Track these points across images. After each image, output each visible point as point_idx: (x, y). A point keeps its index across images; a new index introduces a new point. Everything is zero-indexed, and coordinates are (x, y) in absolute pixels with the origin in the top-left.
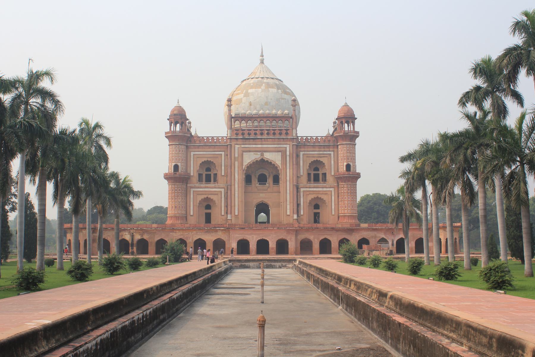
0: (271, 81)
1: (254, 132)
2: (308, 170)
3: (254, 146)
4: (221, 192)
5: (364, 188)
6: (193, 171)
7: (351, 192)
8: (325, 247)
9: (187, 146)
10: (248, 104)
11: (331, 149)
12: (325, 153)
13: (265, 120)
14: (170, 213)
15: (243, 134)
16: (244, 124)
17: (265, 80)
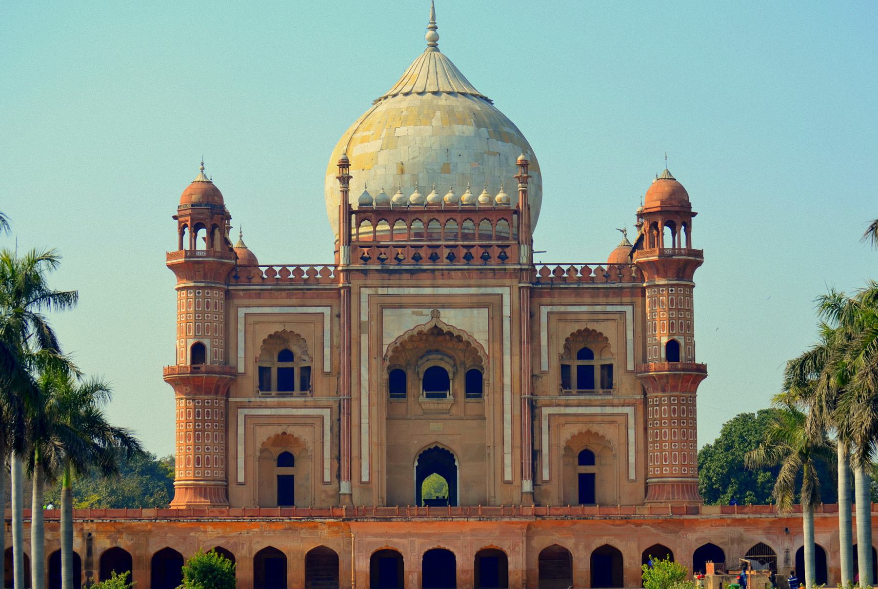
0: (459, 103)
1: (412, 251)
2: (561, 357)
3: (413, 291)
4: (322, 418)
6: (245, 359)
7: (679, 419)
10: (394, 170)
11: (626, 300)
12: (609, 308)
13: (442, 218)
14: (181, 475)
16: (383, 227)
17: (443, 100)
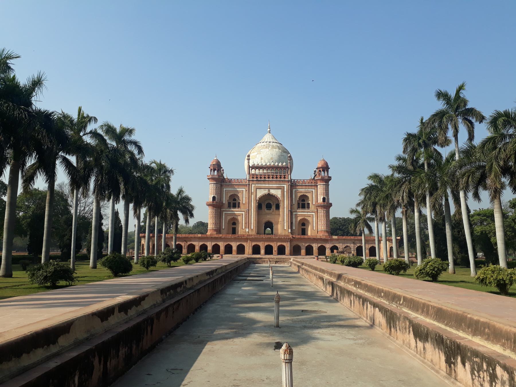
0: (275, 144)
5: (334, 213)
6: (225, 201)
8: (309, 251)
9: (221, 186)
10: (260, 159)
14: (210, 227)
15: (257, 178)
17: (271, 144)
